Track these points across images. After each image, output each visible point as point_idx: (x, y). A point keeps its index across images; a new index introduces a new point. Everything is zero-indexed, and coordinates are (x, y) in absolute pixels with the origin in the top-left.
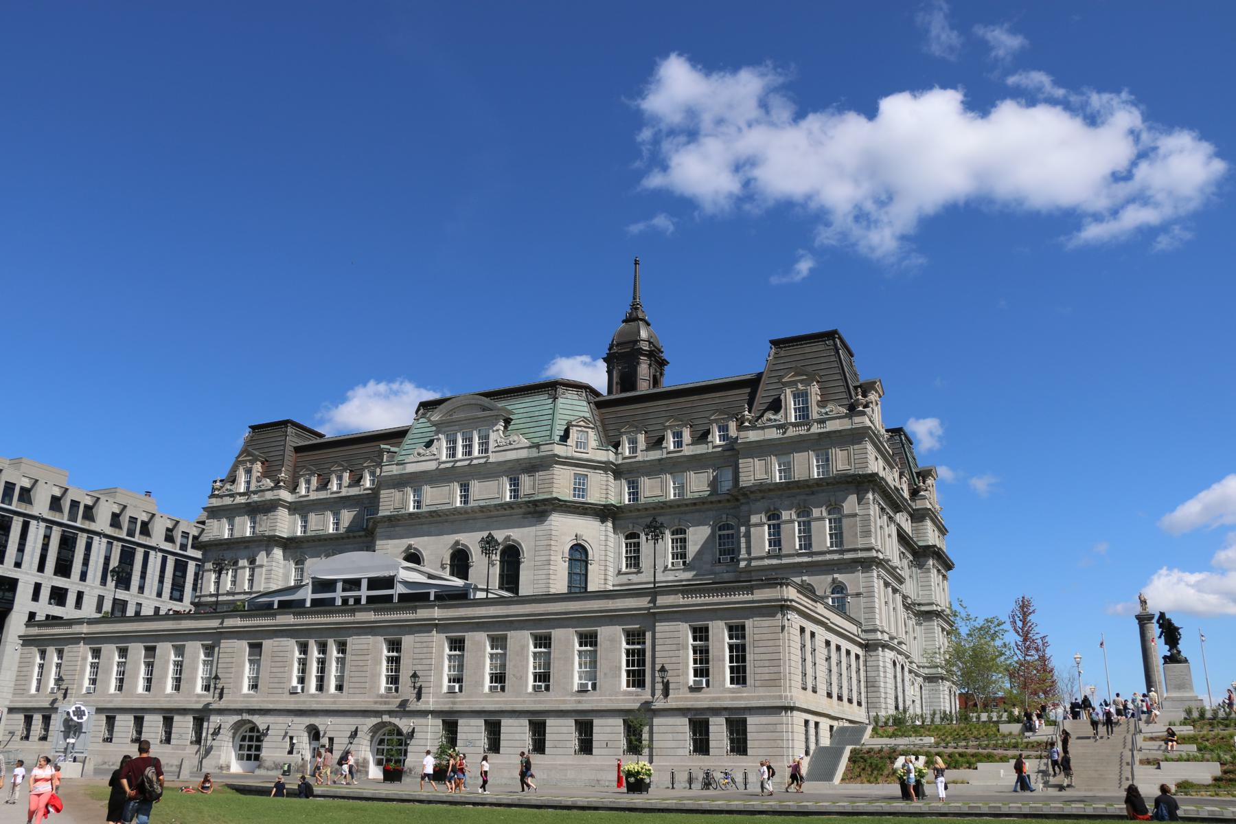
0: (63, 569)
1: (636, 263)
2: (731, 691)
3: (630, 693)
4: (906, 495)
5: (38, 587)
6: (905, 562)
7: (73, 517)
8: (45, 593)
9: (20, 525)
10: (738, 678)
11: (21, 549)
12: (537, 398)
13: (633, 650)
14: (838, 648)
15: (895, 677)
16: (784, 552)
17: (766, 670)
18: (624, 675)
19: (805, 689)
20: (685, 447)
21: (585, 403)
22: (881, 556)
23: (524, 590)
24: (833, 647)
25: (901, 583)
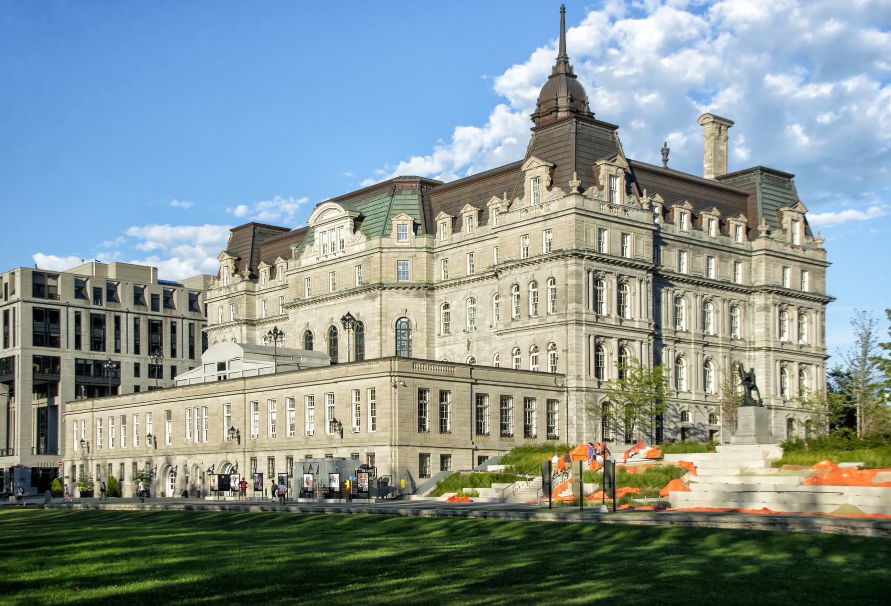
0: (155, 348)
2: (371, 436)
5: (137, 367)
7: (155, 308)
8: (144, 371)
9: (113, 319)
11: (117, 337)
21: (416, 197)
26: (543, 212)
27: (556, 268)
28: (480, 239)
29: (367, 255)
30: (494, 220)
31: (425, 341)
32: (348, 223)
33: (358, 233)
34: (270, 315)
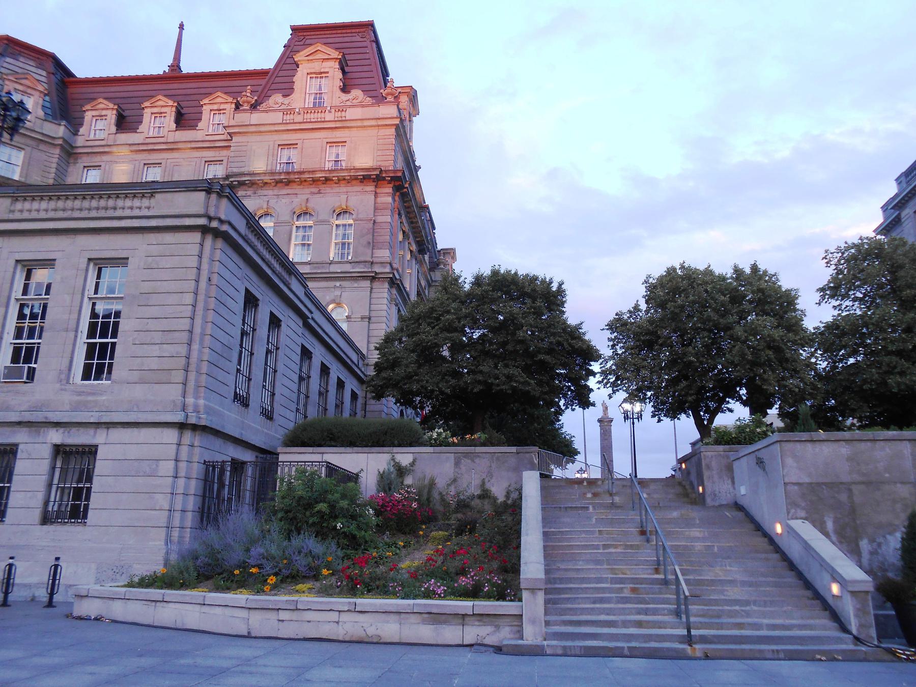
1: (181, 27)
17: (156, 350)
19: (243, 401)
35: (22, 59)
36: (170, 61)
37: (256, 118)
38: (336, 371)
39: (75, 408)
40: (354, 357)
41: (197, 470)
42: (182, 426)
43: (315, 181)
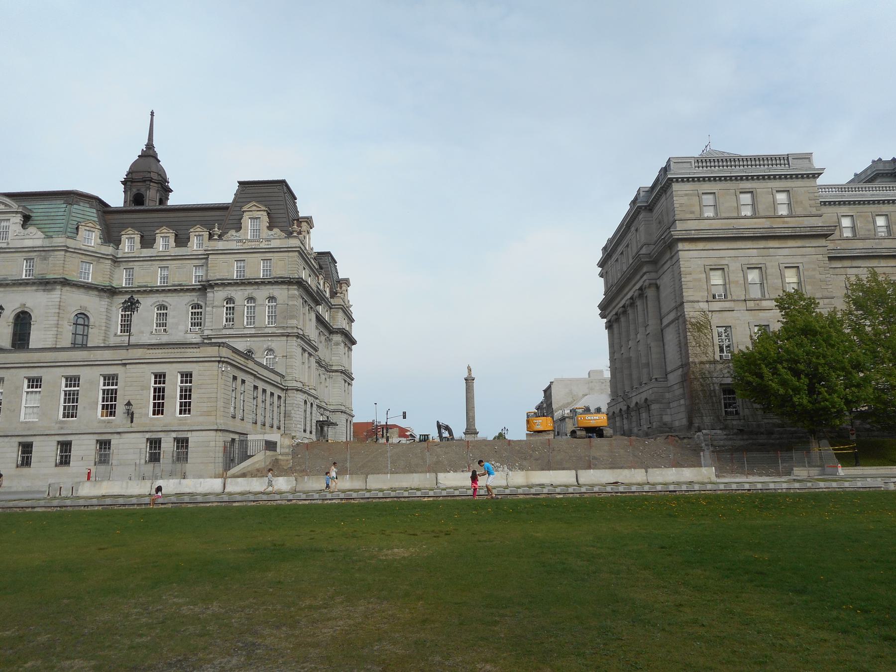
1: (152, 114)
2: (180, 419)
3: (104, 421)
4: (328, 295)
6: (323, 338)
10: (158, 411)
12: (54, 202)
13: (108, 390)
14: (264, 391)
15: (305, 411)
16: (235, 326)
17: (205, 405)
18: (100, 407)
19: (234, 417)
20: (170, 249)
21: (94, 211)
22: (301, 333)
23: (34, 343)
24: (260, 390)
25: (316, 351)
26: (262, 245)
27: (280, 292)
28: (175, 258)
29: (45, 252)
30: (195, 245)
31: (101, 338)
32: (18, 219)
33: (32, 230)
34: (136, 284)
35: (82, 204)
36: (146, 142)
37: (220, 245)
38: (270, 389)
39: (180, 425)
40: (278, 379)
41: (222, 444)
42: (216, 430)
43: (256, 283)
